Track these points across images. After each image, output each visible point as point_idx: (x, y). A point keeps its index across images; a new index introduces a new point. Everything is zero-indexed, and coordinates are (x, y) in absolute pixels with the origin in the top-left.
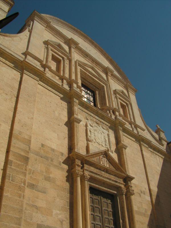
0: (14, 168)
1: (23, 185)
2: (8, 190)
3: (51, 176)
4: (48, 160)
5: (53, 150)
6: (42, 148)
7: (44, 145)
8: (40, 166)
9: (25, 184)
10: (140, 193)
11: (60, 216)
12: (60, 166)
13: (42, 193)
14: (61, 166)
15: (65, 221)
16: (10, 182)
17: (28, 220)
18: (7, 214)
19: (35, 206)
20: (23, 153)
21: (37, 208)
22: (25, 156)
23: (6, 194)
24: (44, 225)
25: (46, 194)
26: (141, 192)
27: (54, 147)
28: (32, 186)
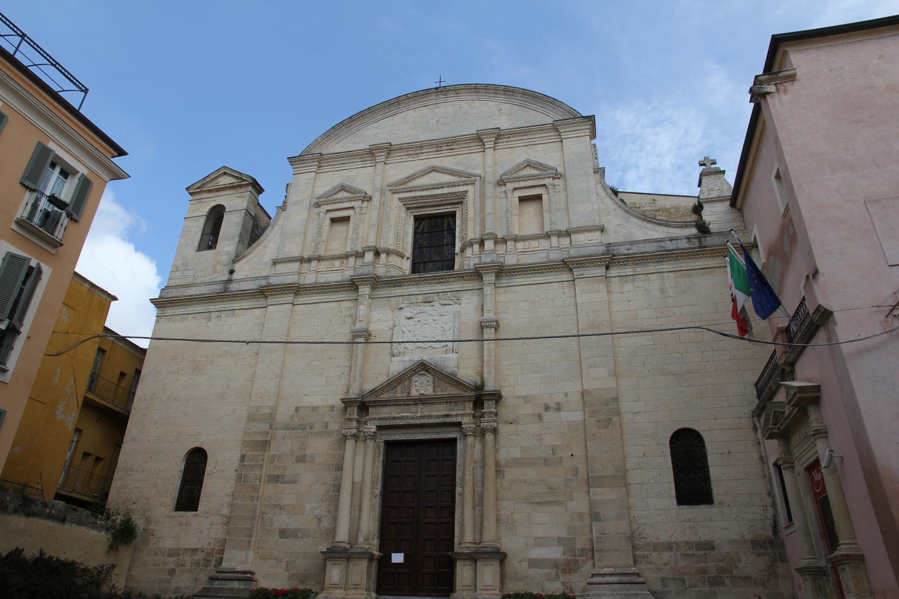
0: (247, 463)
1: (258, 483)
2: (239, 495)
3: (308, 452)
4: (305, 429)
5: (315, 409)
6: (296, 413)
7: (299, 407)
8: (290, 445)
9: (260, 481)
11: (317, 512)
12: (326, 430)
15: (326, 516)
16: (242, 485)
17: (267, 527)
18: (236, 526)
19: (278, 505)
20: (260, 438)
21: (281, 507)
22: (263, 441)
23: (237, 502)
24: (290, 529)
26: (547, 408)
27: (317, 401)
28: (275, 479)
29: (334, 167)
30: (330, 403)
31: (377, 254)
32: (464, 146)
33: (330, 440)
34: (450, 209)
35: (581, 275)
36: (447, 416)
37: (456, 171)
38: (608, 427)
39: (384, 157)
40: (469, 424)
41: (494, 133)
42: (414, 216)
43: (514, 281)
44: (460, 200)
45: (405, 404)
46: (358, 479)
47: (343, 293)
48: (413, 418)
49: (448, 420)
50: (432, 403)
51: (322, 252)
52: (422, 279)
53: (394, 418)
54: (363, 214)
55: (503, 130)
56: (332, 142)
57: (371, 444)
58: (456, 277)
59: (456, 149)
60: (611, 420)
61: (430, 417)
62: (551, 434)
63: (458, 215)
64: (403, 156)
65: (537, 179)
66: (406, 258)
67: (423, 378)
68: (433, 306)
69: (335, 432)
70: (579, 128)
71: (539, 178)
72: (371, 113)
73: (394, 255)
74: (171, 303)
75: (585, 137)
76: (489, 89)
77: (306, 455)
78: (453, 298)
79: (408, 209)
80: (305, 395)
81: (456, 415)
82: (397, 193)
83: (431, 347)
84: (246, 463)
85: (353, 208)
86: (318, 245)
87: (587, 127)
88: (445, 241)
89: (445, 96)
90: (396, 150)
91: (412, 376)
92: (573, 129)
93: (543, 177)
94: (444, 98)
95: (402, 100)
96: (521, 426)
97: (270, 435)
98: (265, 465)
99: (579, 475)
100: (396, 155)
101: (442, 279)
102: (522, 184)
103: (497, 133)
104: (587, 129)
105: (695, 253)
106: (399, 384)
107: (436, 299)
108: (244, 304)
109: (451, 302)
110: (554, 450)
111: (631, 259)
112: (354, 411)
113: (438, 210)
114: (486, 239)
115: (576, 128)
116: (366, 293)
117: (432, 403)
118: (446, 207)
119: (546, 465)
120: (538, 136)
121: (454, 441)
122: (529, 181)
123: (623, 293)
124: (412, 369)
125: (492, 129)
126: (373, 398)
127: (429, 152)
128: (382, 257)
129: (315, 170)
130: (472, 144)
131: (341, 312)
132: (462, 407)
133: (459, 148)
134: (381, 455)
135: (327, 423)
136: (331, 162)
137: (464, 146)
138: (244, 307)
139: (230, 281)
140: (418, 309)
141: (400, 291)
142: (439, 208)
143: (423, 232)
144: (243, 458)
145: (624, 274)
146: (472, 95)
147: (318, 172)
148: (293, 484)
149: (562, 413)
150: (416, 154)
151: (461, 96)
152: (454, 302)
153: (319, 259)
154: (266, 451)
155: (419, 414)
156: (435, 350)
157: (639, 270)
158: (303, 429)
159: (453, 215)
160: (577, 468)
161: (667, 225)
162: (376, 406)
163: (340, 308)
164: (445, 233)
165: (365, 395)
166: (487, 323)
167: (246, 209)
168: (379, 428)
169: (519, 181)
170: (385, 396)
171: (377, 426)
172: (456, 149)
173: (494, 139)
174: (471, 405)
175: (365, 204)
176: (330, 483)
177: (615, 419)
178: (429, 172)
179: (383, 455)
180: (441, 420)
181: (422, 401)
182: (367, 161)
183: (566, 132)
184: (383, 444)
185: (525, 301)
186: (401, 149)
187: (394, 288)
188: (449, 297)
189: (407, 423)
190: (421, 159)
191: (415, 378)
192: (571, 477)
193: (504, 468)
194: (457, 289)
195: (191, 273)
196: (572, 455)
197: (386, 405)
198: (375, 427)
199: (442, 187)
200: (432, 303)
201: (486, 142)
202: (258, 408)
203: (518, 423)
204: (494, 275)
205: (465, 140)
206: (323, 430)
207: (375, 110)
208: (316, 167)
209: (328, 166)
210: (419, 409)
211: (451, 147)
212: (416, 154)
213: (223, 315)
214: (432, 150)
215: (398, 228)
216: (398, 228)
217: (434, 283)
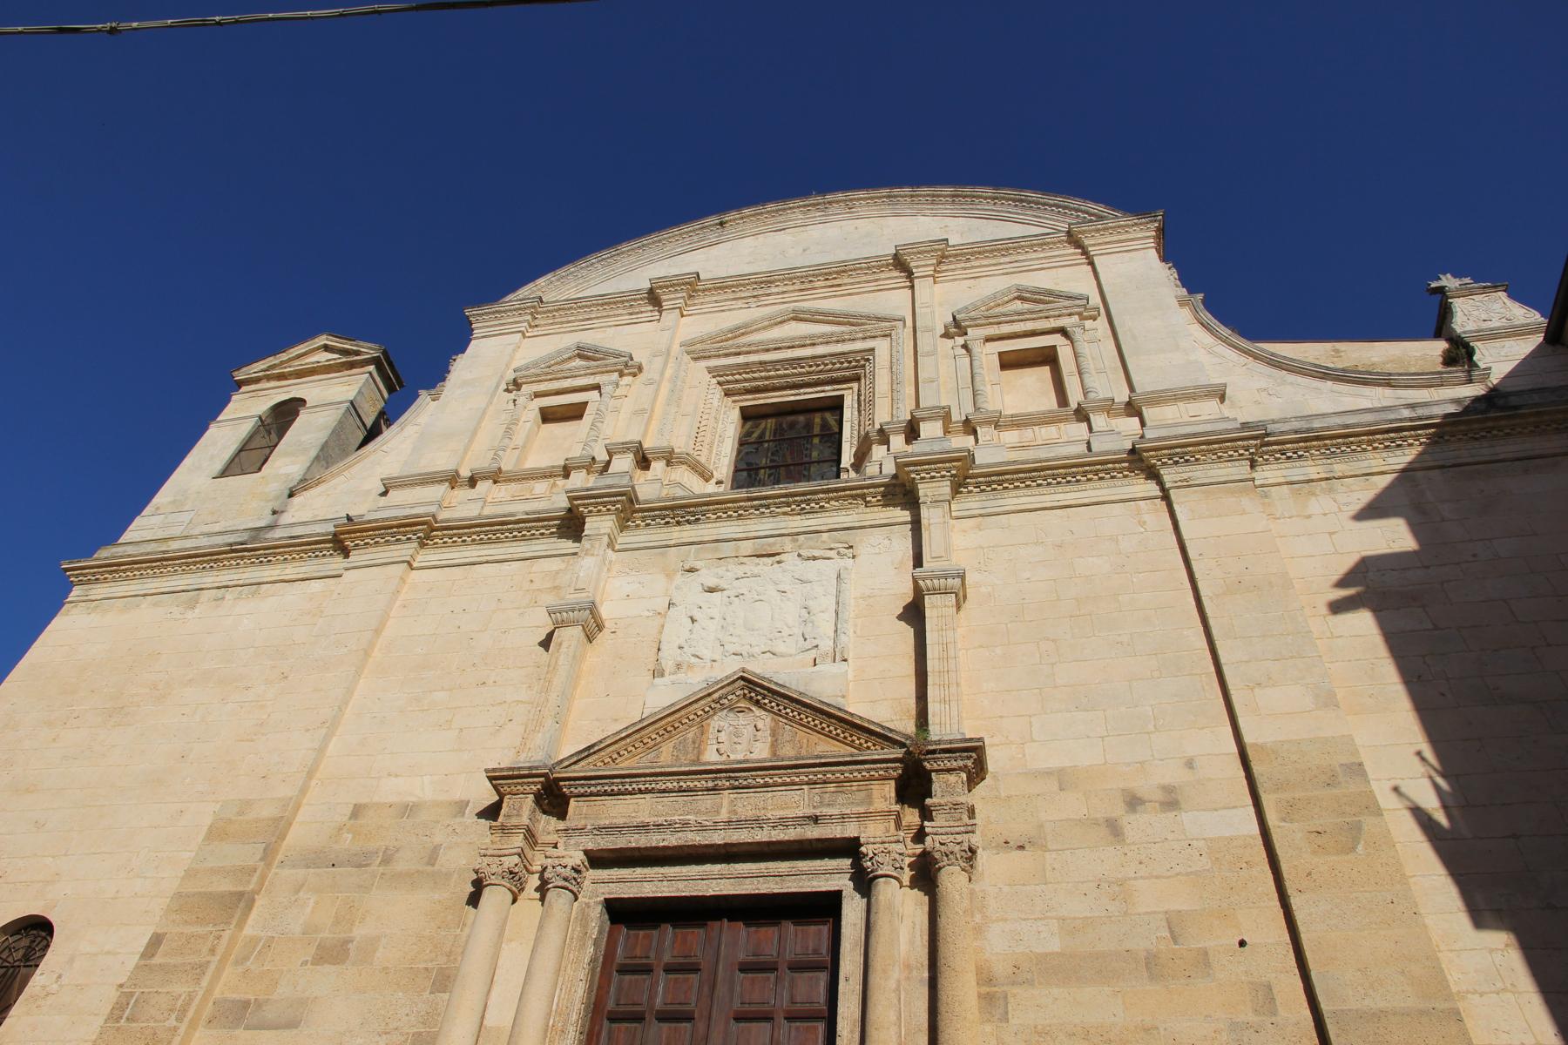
4: (366, 865)
8: (309, 910)
10: (1118, 810)
12: (429, 868)
13: (279, 1032)
14: (433, 865)
20: (226, 886)
22: (231, 893)
25: (295, 1031)
26: (1134, 802)
27: (421, 788)
29: (565, 325)
30: (458, 794)
31: (644, 462)
32: (864, 278)
33: (436, 896)
34: (829, 391)
35: (1186, 480)
36: (815, 819)
37: (846, 316)
38: (1353, 849)
39: (681, 301)
40: (883, 843)
41: (936, 250)
42: (740, 407)
43: (1001, 502)
44: (855, 370)
45: (681, 790)
46: (500, 1016)
47: (545, 541)
48: (702, 828)
49: (813, 832)
50: (766, 785)
51: (507, 465)
52: (755, 503)
53: (643, 827)
54: (620, 397)
55: (954, 246)
56: (568, 290)
57: (559, 899)
58: (845, 498)
59: (846, 285)
60: (1355, 830)
61: (758, 822)
62: (1157, 877)
63: (847, 402)
64: (726, 300)
65: (1041, 318)
66: (713, 481)
67: (742, 719)
68: (779, 562)
69: (455, 876)
70: (1131, 236)
71: (1046, 317)
72: (660, 241)
73: (685, 467)
74: (111, 572)
75: (1145, 251)
76: (920, 196)
77: (352, 941)
78: (832, 546)
79: (727, 394)
80: (389, 775)
81: (843, 816)
82: (705, 358)
83: (769, 651)
84: (157, 960)
85: (597, 387)
86: (500, 453)
87: (1148, 234)
88: (815, 454)
89: (823, 213)
90: (709, 290)
91: (708, 714)
92: (1115, 238)
93: (1057, 313)
94: (819, 216)
95: (730, 221)
96: (1054, 855)
97: (255, 879)
98: (212, 967)
99: (1282, 1012)
100: (707, 299)
101: (808, 502)
102: (1006, 329)
103: (943, 249)
104: (1148, 237)
105: (1490, 424)
106: (667, 732)
107: (788, 547)
108: (287, 571)
109: (832, 554)
110: (1175, 926)
111: (1315, 443)
112: (521, 807)
113: (799, 394)
114: (923, 419)
115: (1123, 237)
116: (602, 531)
117: (766, 785)
118: (819, 389)
119: (1152, 978)
120: (1034, 255)
121: (826, 907)
122: (1022, 324)
123: (1309, 517)
124: (709, 695)
125: (930, 241)
126: (578, 770)
127: (784, 292)
128: (655, 468)
129: (523, 329)
130: (883, 276)
131: (532, 581)
132: (863, 794)
133: (852, 284)
134: (590, 942)
135: (436, 849)
136: (561, 316)
137: (864, 278)
138: (286, 578)
139: (271, 527)
140: (740, 571)
141: (693, 533)
142: (802, 391)
143: (760, 441)
144: (156, 941)
145: (1302, 478)
146: (882, 210)
147: (527, 335)
148: (286, 1033)
149: (1186, 818)
150: (754, 297)
151: (858, 212)
152: (838, 553)
153: (496, 477)
154: (228, 923)
155: (724, 815)
156: (781, 660)
157: (1339, 468)
158: (360, 866)
159: (836, 405)
160: (1269, 988)
161: (1389, 385)
162: (592, 794)
163: (530, 573)
164: (816, 441)
165: (562, 761)
166: (935, 581)
167: (352, 403)
168: (597, 860)
169: (1000, 323)
170: (625, 765)
171: (586, 852)
172: (846, 285)
173: (935, 261)
174: (890, 789)
175: (627, 380)
176: (406, 1030)
177: (1368, 822)
178: (781, 322)
179: (596, 943)
180: (791, 834)
181: (734, 776)
182: (642, 312)
183: (1099, 244)
184: (600, 908)
185: (1035, 544)
186: (720, 288)
187: (678, 528)
188: (824, 542)
189: (681, 843)
190: (766, 305)
191: (717, 722)
192: (1252, 1018)
193: (1005, 988)
194: (845, 525)
195: (186, 517)
196: (1242, 944)
197: (620, 793)
198: (581, 856)
199: (814, 344)
200: (777, 558)
201: (917, 267)
202: (248, 803)
203: (1044, 848)
204: (948, 483)
205: (868, 268)
206: (421, 869)
207: (670, 237)
208: (526, 324)
209: (552, 324)
210: (725, 802)
211: (835, 282)
212: (754, 297)
213: (230, 595)
214: (791, 288)
215: (700, 419)
216: (700, 419)
217: (785, 514)
